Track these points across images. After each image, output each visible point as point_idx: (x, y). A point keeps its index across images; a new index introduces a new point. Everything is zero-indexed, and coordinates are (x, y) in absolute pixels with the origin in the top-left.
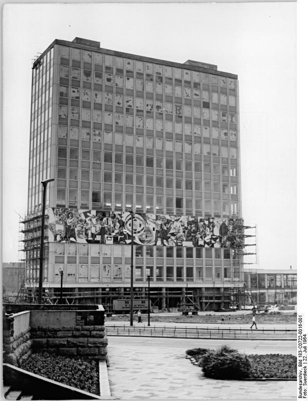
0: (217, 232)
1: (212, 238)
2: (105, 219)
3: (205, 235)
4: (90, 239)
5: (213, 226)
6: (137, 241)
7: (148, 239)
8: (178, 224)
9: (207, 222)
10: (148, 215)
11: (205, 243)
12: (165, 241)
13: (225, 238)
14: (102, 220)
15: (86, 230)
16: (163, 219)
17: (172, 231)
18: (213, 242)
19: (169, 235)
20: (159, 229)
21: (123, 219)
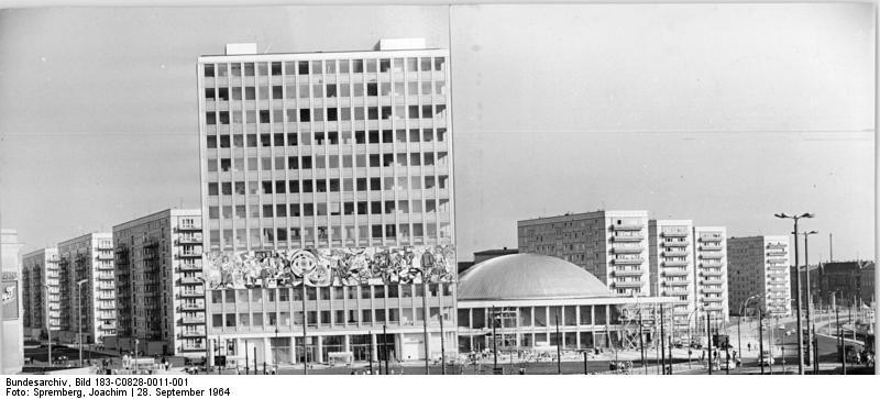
0: (417, 263)
1: (410, 272)
2: (266, 260)
3: (400, 269)
4: (249, 283)
5: (412, 257)
6: (307, 282)
7: (321, 279)
8: (362, 258)
9: (402, 253)
10: (321, 250)
11: (400, 278)
12: (344, 280)
13: (430, 270)
14: (262, 261)
15: (245, 274)
16: (339, 253)
17: (352, 268)
18: (411, 276)
19: (349, 273)
20: (335, 266)
21: (288, 258)
